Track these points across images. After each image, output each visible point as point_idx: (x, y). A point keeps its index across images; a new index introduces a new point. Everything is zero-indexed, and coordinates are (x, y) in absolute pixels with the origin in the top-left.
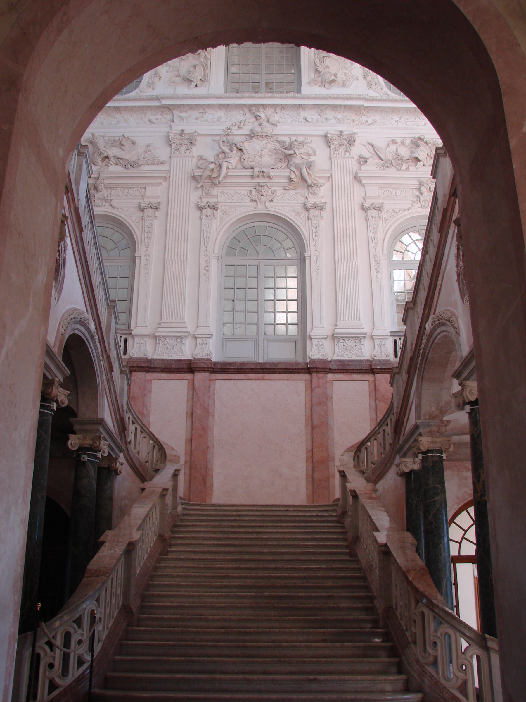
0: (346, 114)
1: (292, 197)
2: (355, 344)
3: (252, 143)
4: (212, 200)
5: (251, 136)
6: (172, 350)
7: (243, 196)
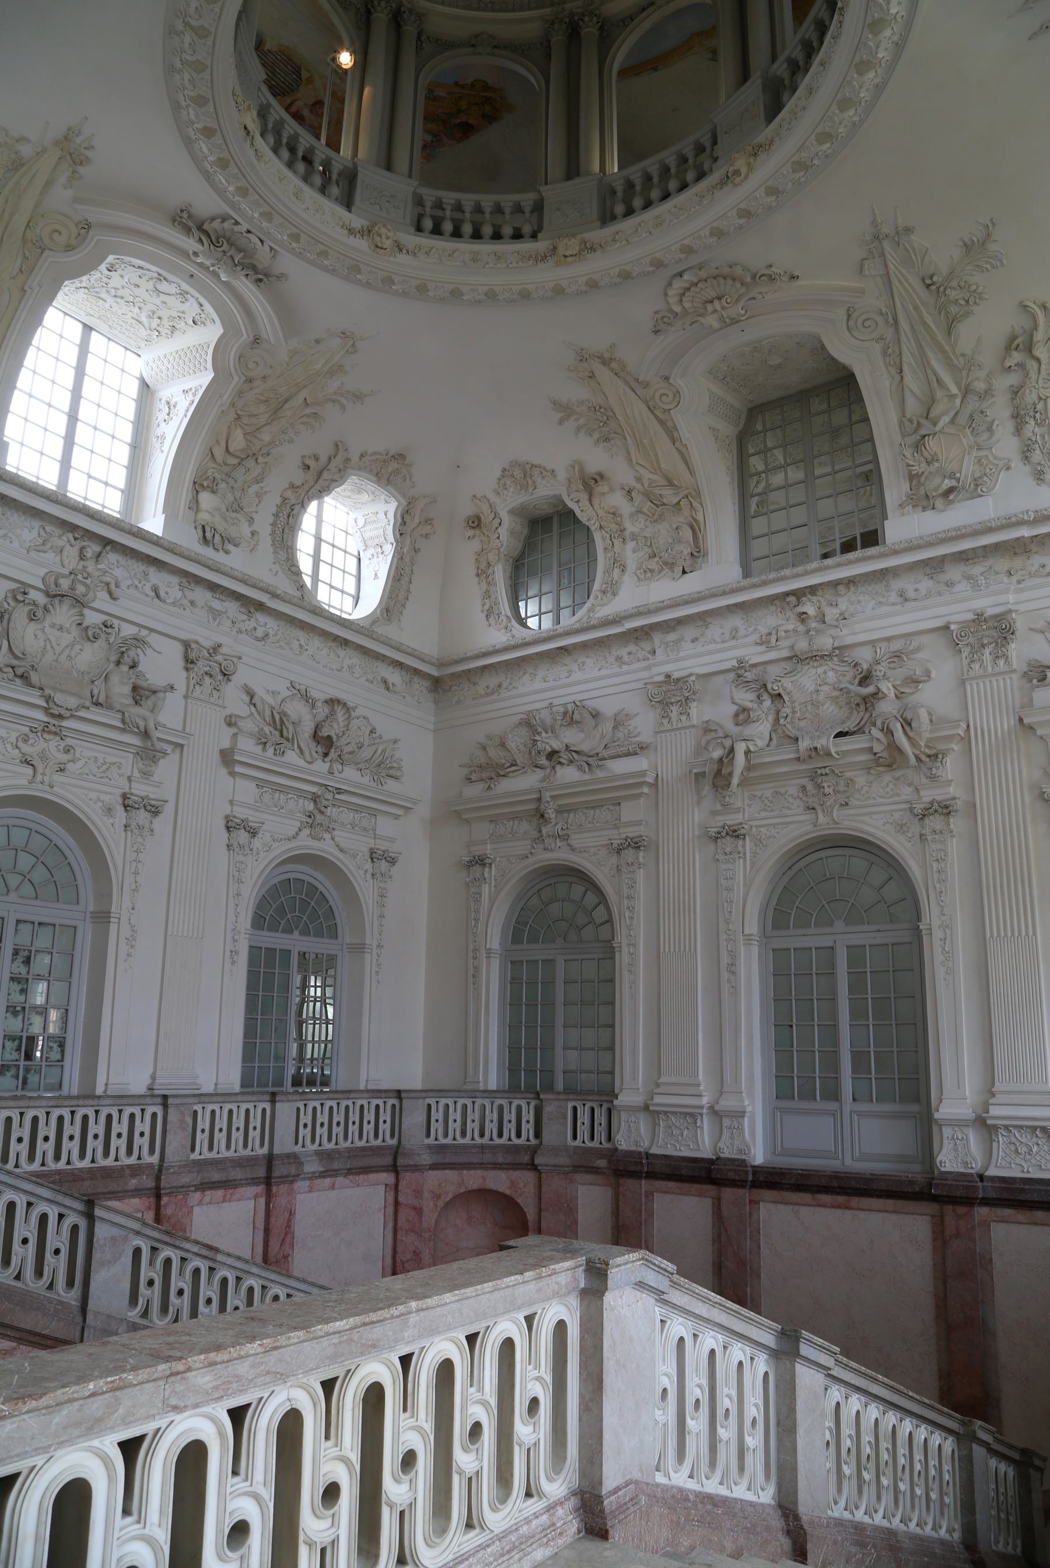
0: (990, 561)
1: (888, 789)
2: (1034, 1140)
3: (800, 675)
4: (732, 819)
5: (797, 659)
6: (680, 1138)
7: (791, 800)
